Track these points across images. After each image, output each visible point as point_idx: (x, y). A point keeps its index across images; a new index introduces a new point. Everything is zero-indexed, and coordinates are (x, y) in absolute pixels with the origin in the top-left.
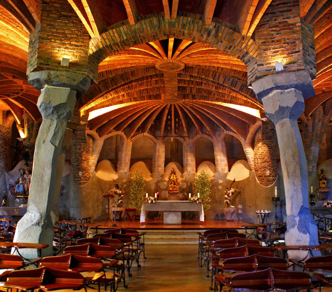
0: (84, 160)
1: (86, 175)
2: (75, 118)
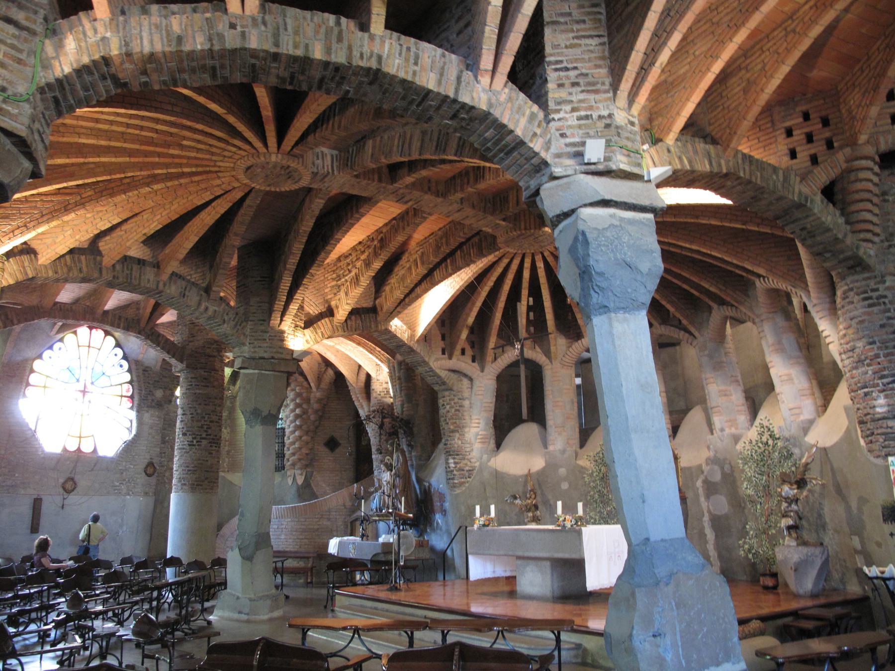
0: (453, 431)
1: (461, 465)
2: (260, 347)
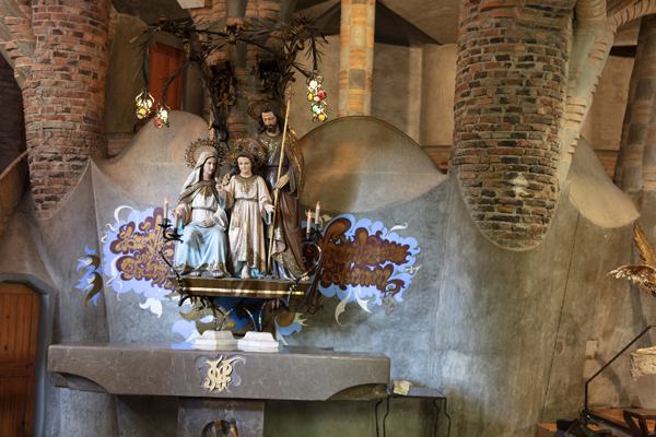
0: (541, 121)
